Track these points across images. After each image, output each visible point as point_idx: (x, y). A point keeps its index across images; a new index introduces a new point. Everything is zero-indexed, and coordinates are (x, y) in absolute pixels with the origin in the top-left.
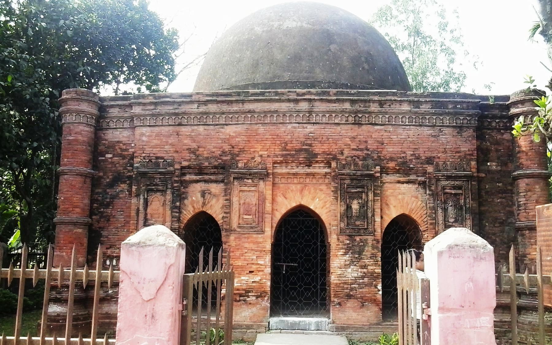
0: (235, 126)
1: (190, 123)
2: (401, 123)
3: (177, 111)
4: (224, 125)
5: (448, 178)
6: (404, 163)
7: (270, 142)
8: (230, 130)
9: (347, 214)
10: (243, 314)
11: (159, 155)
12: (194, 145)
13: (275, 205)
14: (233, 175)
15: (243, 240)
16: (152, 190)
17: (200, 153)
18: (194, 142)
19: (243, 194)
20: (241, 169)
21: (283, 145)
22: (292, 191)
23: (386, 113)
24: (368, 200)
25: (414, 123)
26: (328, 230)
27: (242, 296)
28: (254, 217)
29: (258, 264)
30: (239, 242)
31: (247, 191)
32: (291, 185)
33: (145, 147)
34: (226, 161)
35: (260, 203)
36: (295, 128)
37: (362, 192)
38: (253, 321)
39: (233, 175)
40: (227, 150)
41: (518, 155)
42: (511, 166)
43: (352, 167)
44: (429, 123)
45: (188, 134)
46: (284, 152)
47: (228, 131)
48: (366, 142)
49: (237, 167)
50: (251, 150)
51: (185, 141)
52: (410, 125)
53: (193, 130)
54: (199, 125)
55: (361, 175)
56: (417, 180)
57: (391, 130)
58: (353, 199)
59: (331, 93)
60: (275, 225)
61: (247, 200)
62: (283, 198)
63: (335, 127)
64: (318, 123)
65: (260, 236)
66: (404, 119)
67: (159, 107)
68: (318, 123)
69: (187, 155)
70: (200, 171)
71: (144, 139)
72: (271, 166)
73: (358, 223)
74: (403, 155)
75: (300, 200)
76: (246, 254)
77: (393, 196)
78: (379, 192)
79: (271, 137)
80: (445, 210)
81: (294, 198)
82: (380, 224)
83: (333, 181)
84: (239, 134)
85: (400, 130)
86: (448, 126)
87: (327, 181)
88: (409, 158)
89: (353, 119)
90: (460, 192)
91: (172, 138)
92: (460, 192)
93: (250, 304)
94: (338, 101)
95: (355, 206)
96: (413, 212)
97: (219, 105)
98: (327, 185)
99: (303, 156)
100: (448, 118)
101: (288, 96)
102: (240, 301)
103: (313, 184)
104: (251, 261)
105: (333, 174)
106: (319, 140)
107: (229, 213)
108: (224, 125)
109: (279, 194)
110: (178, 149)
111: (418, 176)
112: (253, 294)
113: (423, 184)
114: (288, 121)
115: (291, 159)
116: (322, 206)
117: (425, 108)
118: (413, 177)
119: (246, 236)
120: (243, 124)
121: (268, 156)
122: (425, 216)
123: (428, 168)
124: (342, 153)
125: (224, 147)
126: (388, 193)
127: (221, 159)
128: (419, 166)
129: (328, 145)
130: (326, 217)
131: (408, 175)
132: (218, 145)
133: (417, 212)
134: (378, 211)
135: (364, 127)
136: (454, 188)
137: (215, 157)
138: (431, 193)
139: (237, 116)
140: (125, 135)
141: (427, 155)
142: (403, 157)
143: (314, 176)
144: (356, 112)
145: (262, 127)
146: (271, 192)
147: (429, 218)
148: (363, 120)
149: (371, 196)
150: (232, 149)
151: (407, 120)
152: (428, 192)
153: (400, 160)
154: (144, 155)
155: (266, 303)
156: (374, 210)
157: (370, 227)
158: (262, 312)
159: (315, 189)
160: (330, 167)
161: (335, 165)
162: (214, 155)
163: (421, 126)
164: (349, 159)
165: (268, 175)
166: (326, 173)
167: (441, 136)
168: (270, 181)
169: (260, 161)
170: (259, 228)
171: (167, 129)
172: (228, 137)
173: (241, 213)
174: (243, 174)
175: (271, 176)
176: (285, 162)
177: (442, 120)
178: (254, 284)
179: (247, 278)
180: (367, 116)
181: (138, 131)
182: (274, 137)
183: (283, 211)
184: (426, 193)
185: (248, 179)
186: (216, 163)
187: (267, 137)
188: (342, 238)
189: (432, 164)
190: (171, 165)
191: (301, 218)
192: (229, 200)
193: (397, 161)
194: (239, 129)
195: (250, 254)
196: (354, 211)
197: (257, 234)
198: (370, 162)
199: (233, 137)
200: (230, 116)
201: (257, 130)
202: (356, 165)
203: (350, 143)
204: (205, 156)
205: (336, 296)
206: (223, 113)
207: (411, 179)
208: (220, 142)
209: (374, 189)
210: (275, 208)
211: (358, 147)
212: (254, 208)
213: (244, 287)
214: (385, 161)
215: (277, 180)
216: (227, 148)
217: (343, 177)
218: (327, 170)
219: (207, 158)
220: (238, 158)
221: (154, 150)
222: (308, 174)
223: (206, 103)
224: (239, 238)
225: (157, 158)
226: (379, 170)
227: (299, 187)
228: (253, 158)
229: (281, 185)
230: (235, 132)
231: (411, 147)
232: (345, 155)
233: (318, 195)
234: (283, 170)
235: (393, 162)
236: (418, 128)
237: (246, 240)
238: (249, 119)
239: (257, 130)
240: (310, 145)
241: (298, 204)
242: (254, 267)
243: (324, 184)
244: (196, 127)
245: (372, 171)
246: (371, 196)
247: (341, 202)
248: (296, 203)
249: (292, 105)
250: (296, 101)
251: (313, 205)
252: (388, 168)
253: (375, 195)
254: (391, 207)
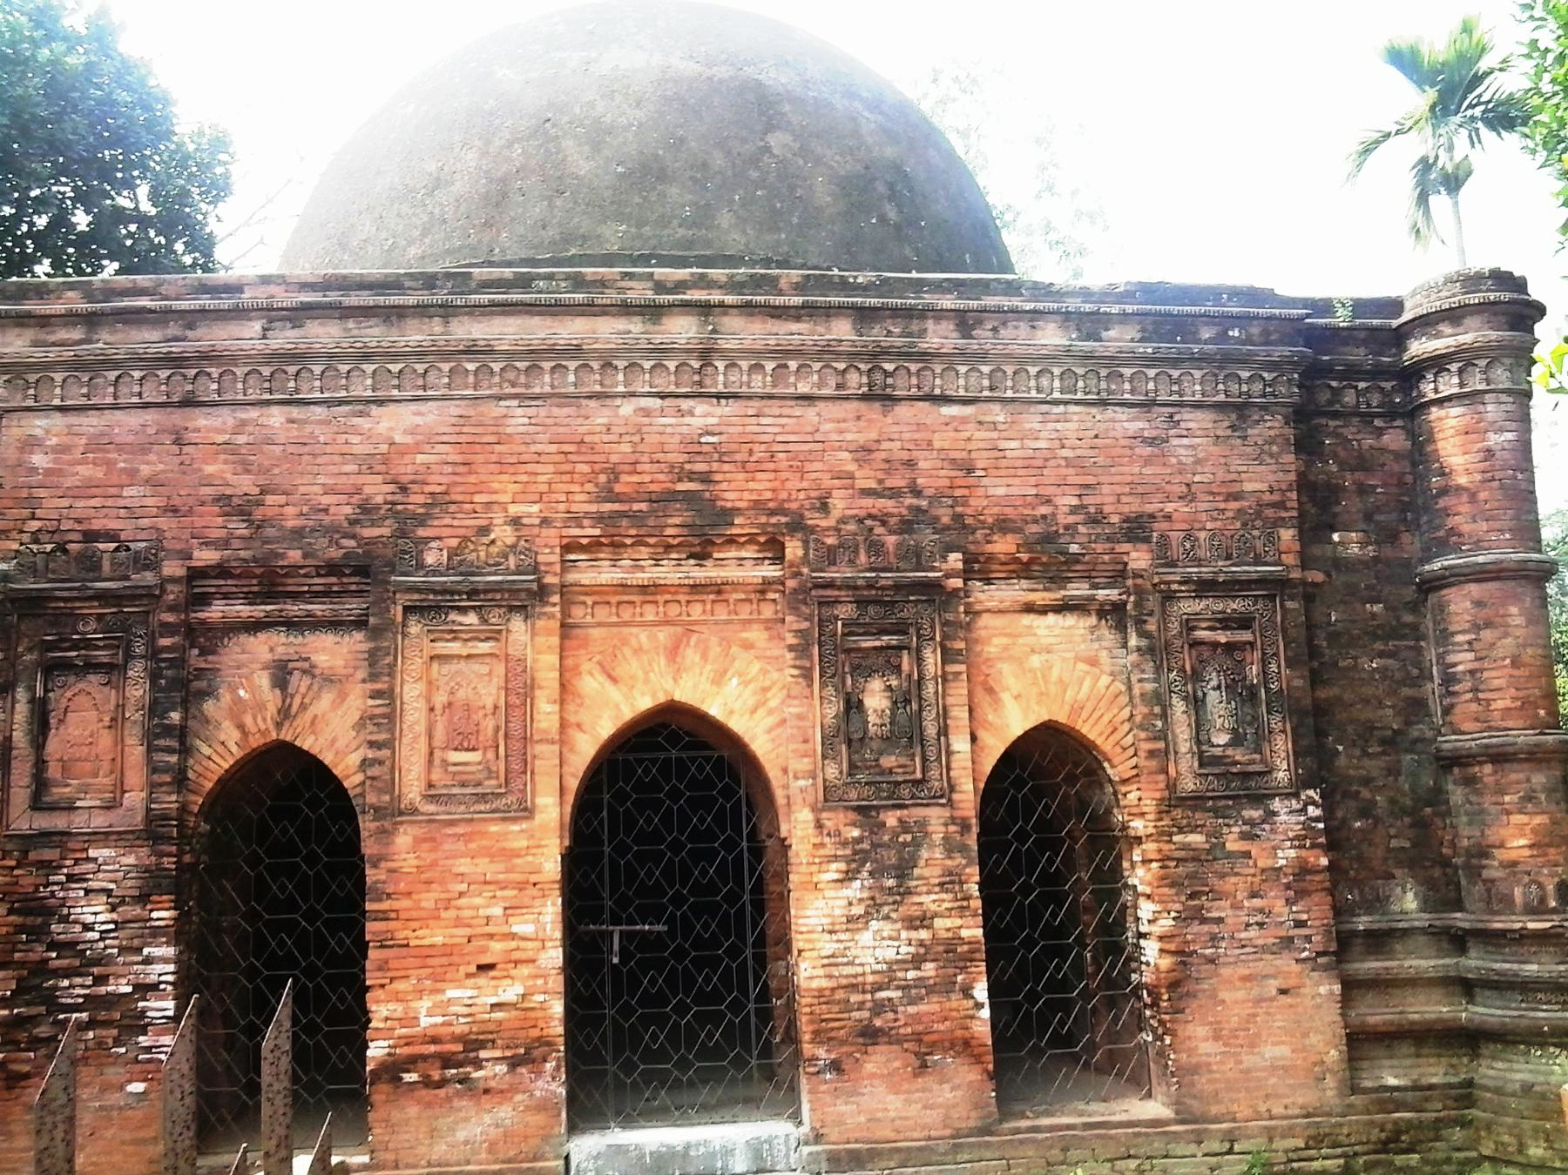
0: (413, 407)
1: (227, 397)
2: (1033, 393)
3: (176, 348)
4: (368, 402)
5: (1204, 588)
6: (1049, 538)
7: (551, 468)
8: (395, 423)
9: (848, 729)
10: (461, 1135)
11: (97, 525)
12: (245, 484)
13: (571, 707)
14: (403, 599)
15: (447, 847)
16: (66, 666)
17: (270, 512)
18: (248, 472)
19: (445, 669)
20: (435, 573)
21: (603, 478)
22: (638, 651)
23: (983, 357)
24: (921, 678)
25: (1080, 396)
26: (779, 795)
27: (449, 1064)
28: (491, 755)
29: (513, 936)
30: (433, 856)
31: (459, 657)
32: (634, 630)
33: (42, 493)
34: (372, 541)
35: (514, 700)
36: (647, 412)
37: (900, 648)
38: (501, 1156)
39: (403, 599)
40: (379, 499)
41: (1442, 503)
42: (1411, 544)
43: (863, 558)
44: (1132, 392)
45: (220, 439)
46: (607, 507)
47: (383, 427)
48: (910, 464)
49: (421, 565)
50: (477, 498)
51: (210, 469)
52: (1066, 403)
53: (243, 423)
54: (268, 403)
55: (897, 587)
56: (1092, 599)
57: (1001, 418)
58: (870, 673)
59: (783, 283)
60: (573, 784)
61: (461, 694)
62: (601, 678)
63: (798, 411)
64: (735, 396)
65: (516, 828)
66: (1045, 382)
67: (104, 335)
68: (735, 396)
69: (214, 523)
70: (269, 583)
72: (556, 558)
73: (888, 761)
74: (1044, 510)
75: (668, 684)
76: (463, 901)
77: (1011, 659)
78: (962, 645)
79: (553, 448)
80: (1197, 704)
81: (647, 681)
82: (968, 763)
83: (794, 610)
84: (429, 440)
85: (1031, 421)
86: (1197, 406)
87: (768, 611)
88: (1065, 519)
89: (865, 380)
90: (1246, 636)
91: (152, 457)
92: (1246, 636)
93: (486, 1091)
94: (808, 311)
95: (876, 699)
96: (1084, 715)
97: (351, 324)
98: (768, 624)
99: (677, 521)
100: (1198, 374)
101: (622, 290)
102: (442, 1083)
103: (716, 623)
104: (477, 931)
105: (791, 584)
106: (738, 457)
107: (389, 744)
108: (368, 402)
109: (586, 666)
110: (176, 501)
111: (1095, 586)
112: (498, 1054)
113: (1114, 614)
114: (621, 389)
115: (633, 532)
116: (751, 702)
117: (1119, 338)
118: (1078, 590)
119: (459, 830)
120: (444, 398)
121: (545, 522)
122: (1126, 726)
123: (1134, 555)
124: (824, 507)
125: (367, 490)
126: (992, 650)
127: (354, 537)
128: (1099, 548)
129: (771, 476)
130: (770, 746)
131: (1057, 580)
132: (344, 479)
133: (1095, 716)
134: (960, 714)
135: (903, 411)
136: (1225, 623)
137: (332, 531)
138: (1144, 643)
139: (420, 368)
141: (1126, 509)
142: (1044, 517)
143: (719, 592)
144: (877, 355)
145: (520, 411)
146: (554, 659)
147: (1143, 735)
148: (899, 383)
149: (932, 659)
150: (398, 497)
151: (1057, 384)
152: (1133, 641)
153: (1034, 528)
155: (551, 1084)
156: (945, 713)
157: (934, 773)
158: (536, 1119)
159: (726, 643)
160: (779, 558)
161: (800, 553)
162: (327, 519)
163: (1103, 403)
164: (852, 527)
165: (542, 593)
166: (767, 584)
167: (1175, 442)
168: (552, 616)
169: (510, 541)
170: (510, 799)
171: (134, 419)
172: (384, 448)
173: (437, 743)
174: (444, 592)
175: (556, 599)
176: (610, 544)
177: (1178, 381)
178: (499, 1015)
179: (470, 993)
180: (913, 367)
182: (566, 448)
183: (606, 728)
184: (1125, 645)
185: (463, 610)
186: (335, 553)
187: (539, 448)
188: (832, 820)
189: (1147, 540)
190: (148, 561)
191: (674, 754)
192: (388, 695)
193: (1019, 531)
194: (430, 418)
195: (478, 901)
196: (872, 719)
197: (504, 819)
198: (927, 537)
199: (404, 450)
200: (395, 368)
201: (499, 421)
202: (875, 547)
203: (852, 467)
204: (290, 524)
205: (819, 1037)
206: (367, 357)
207: (1072, 598)
208: (354, 468)
209: (945, 637)
210: (572, 719)
211: (880, 481)
212: (489, 725)
213: (458, 1030)
214: (979, 534)
215: (578, 613)
216: (378, 490)
217: (829, 592)
218: (771, 571)
219: (298, 533)
220: (421, 532)
221: (80, 504)
222: (696, 588)
223: (298, 315)
224: (433, 840)
225: (90, 536)
226: (960, 565)
227: (663, 634)
228: (484, 530)
229: (595, 633)
230: (412, 432)
231: (1070, 480)
232: (836, 514)
233: (737, 664)
234: (606, 574)
235: (1009, 537)
236: (1094, 410)
237: (461, 846)
238: (471, 379)
239: (499, 421)
240: (705, 478)
241: (662, 699)
242: (497, 946)
243: (758, 621)
244: (253, 413)
245: (933, 569)
246: (932, 659)
247: (823, 686)
248: (654, 695)
249: (636, 326)
250: (653, 312)
251: (719, 700)
252: (991, 558)
253: (948, 656)
254: (1006, 697)
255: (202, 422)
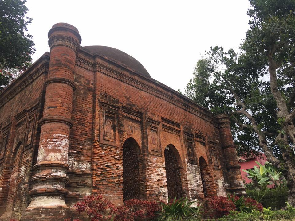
8: (143, 93)
12: (128, 96)
47: (142, 94)
51: (124, 92)
71: (102, 80)
135: (187, 112)
140: (87, 74)
154: (103, 91)
171: (114, 80)
181: (99, 74)
255: (122, 84)
